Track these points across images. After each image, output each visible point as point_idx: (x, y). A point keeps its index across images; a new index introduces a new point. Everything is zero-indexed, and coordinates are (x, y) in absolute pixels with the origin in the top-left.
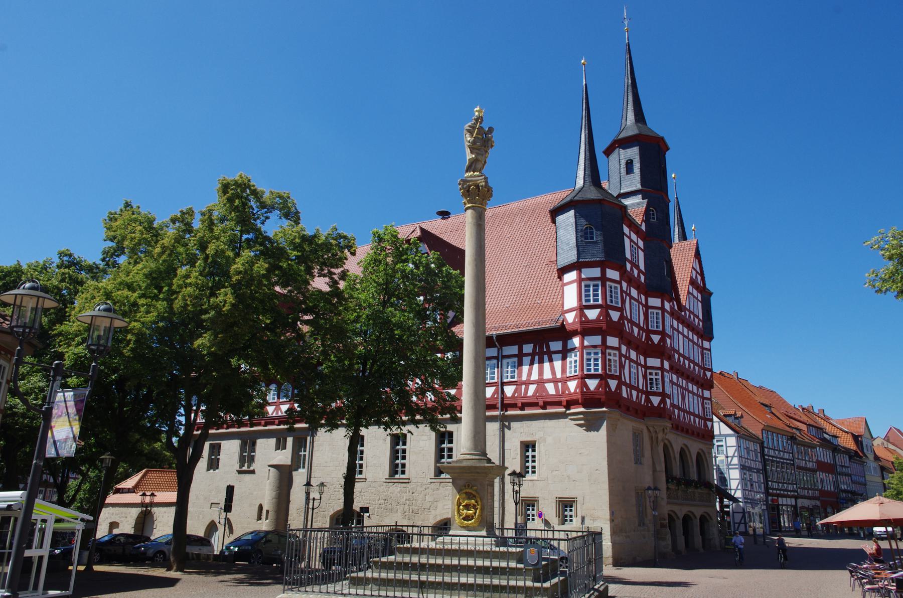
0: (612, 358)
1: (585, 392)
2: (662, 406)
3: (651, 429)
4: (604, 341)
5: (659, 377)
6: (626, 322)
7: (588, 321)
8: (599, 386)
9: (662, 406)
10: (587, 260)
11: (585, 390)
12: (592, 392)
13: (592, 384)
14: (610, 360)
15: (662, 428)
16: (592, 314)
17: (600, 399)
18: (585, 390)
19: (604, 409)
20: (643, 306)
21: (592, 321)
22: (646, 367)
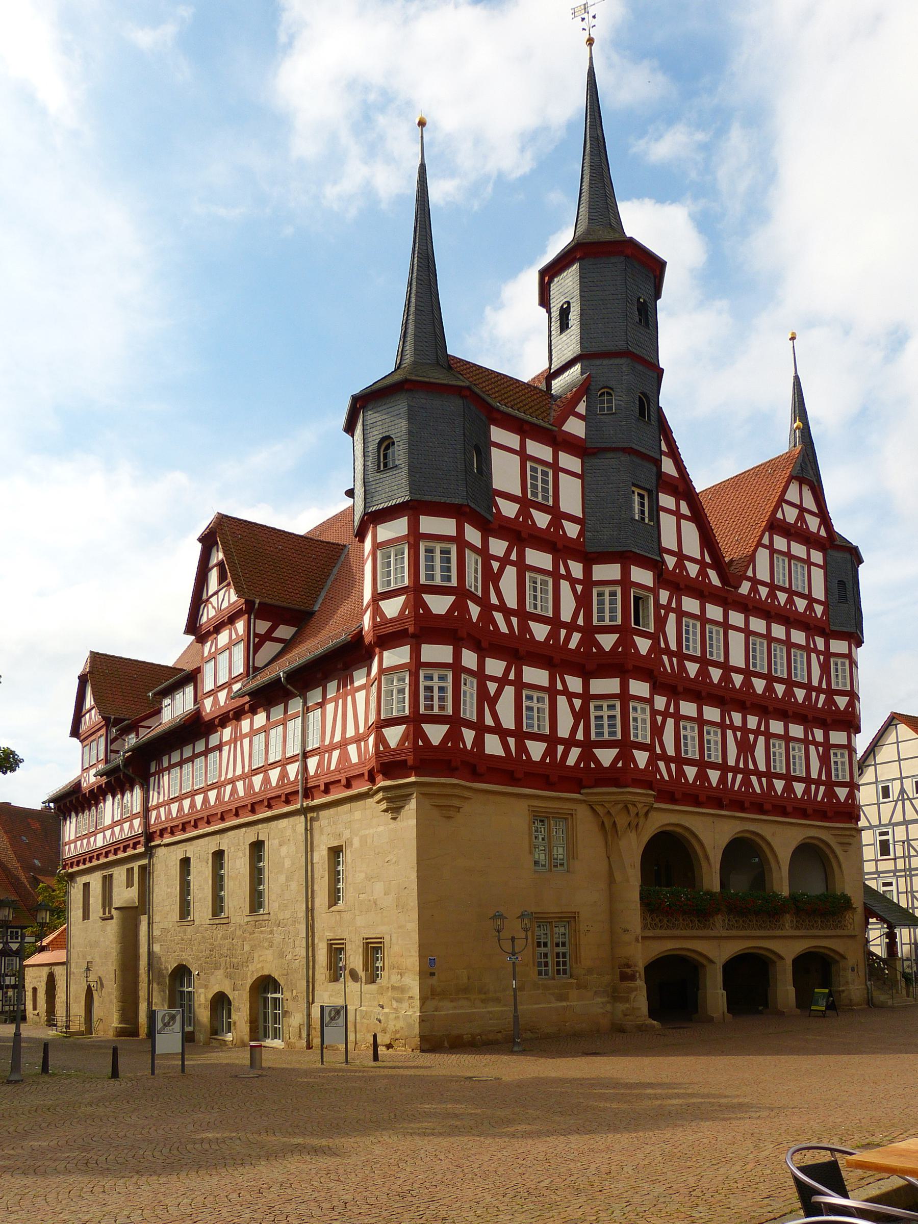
0: (436, 684)
1: (382, 752)
2: (620, 765)
3: (598, 808)
4: (416, 653)
5: (617, 712)
6: (499, 617)
7: (386, 622)
8: (405, 737)
9: (620, 765)
10: (381, 507)
11: (381, 748)
12: (394, 750)
13: (394, 735)
14: (429, 689)
15: (620, 806)
16: (392, 608)
17: (406, 761)
18: (381, 748)
19: (412, 779)
20: (573, 582)
21: (392, 620)
22: (586, 696)
